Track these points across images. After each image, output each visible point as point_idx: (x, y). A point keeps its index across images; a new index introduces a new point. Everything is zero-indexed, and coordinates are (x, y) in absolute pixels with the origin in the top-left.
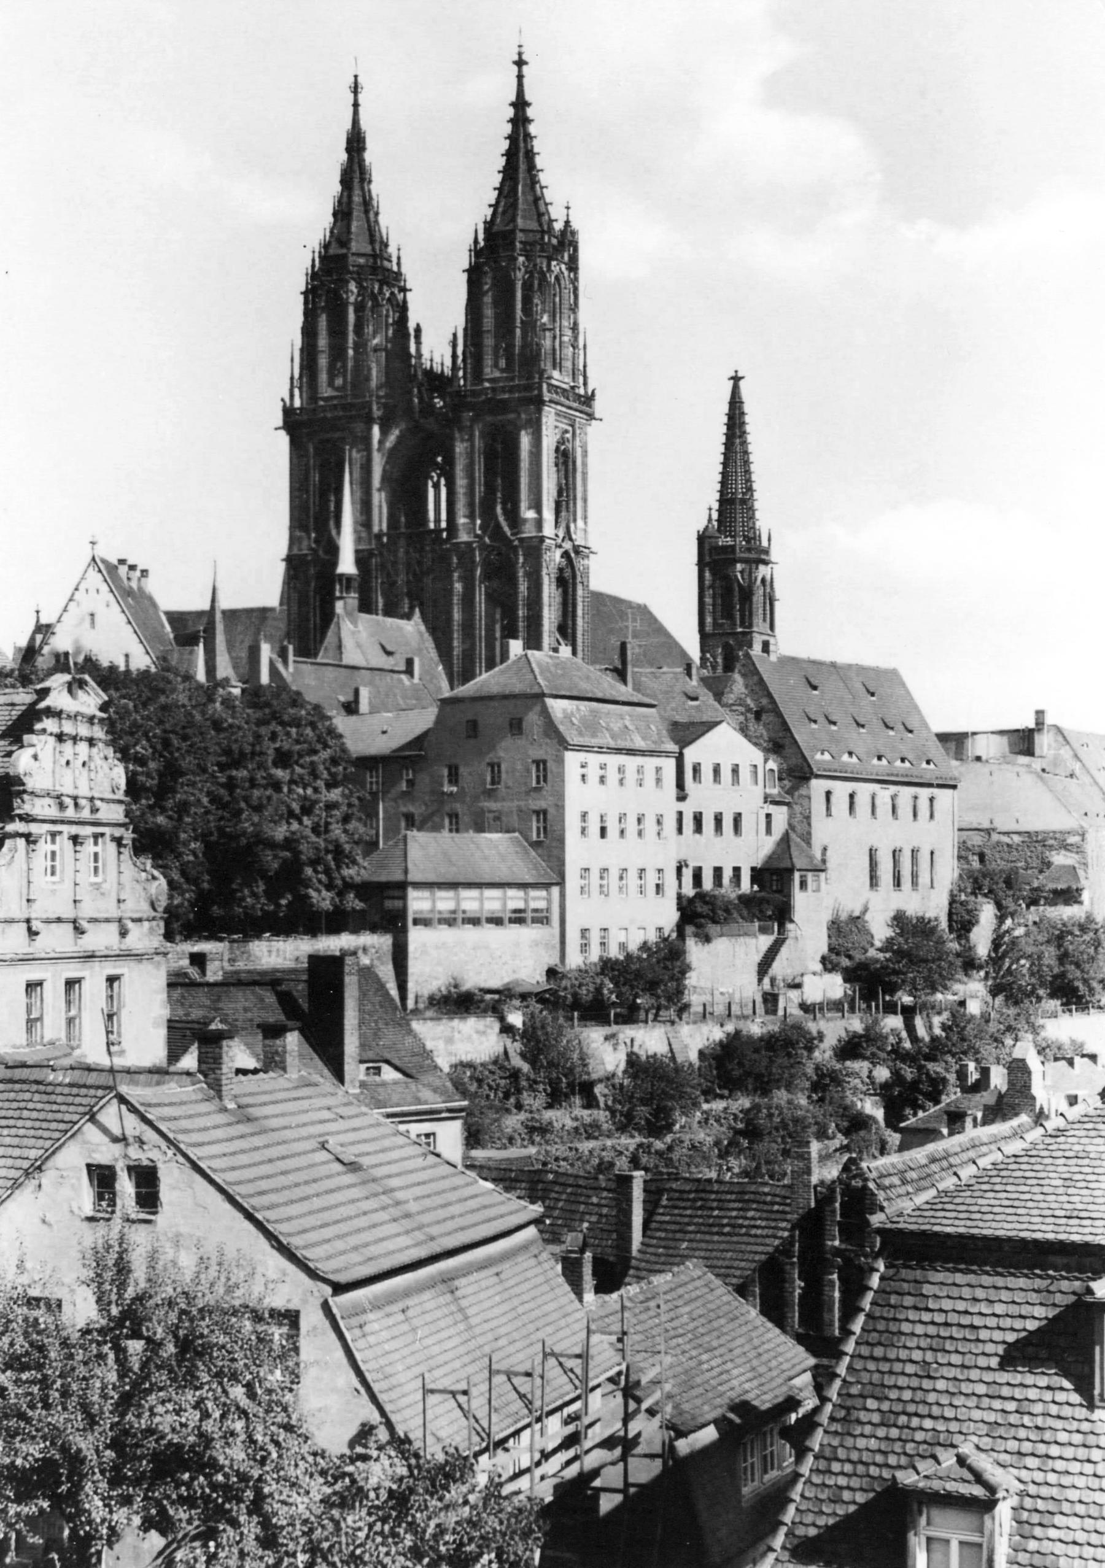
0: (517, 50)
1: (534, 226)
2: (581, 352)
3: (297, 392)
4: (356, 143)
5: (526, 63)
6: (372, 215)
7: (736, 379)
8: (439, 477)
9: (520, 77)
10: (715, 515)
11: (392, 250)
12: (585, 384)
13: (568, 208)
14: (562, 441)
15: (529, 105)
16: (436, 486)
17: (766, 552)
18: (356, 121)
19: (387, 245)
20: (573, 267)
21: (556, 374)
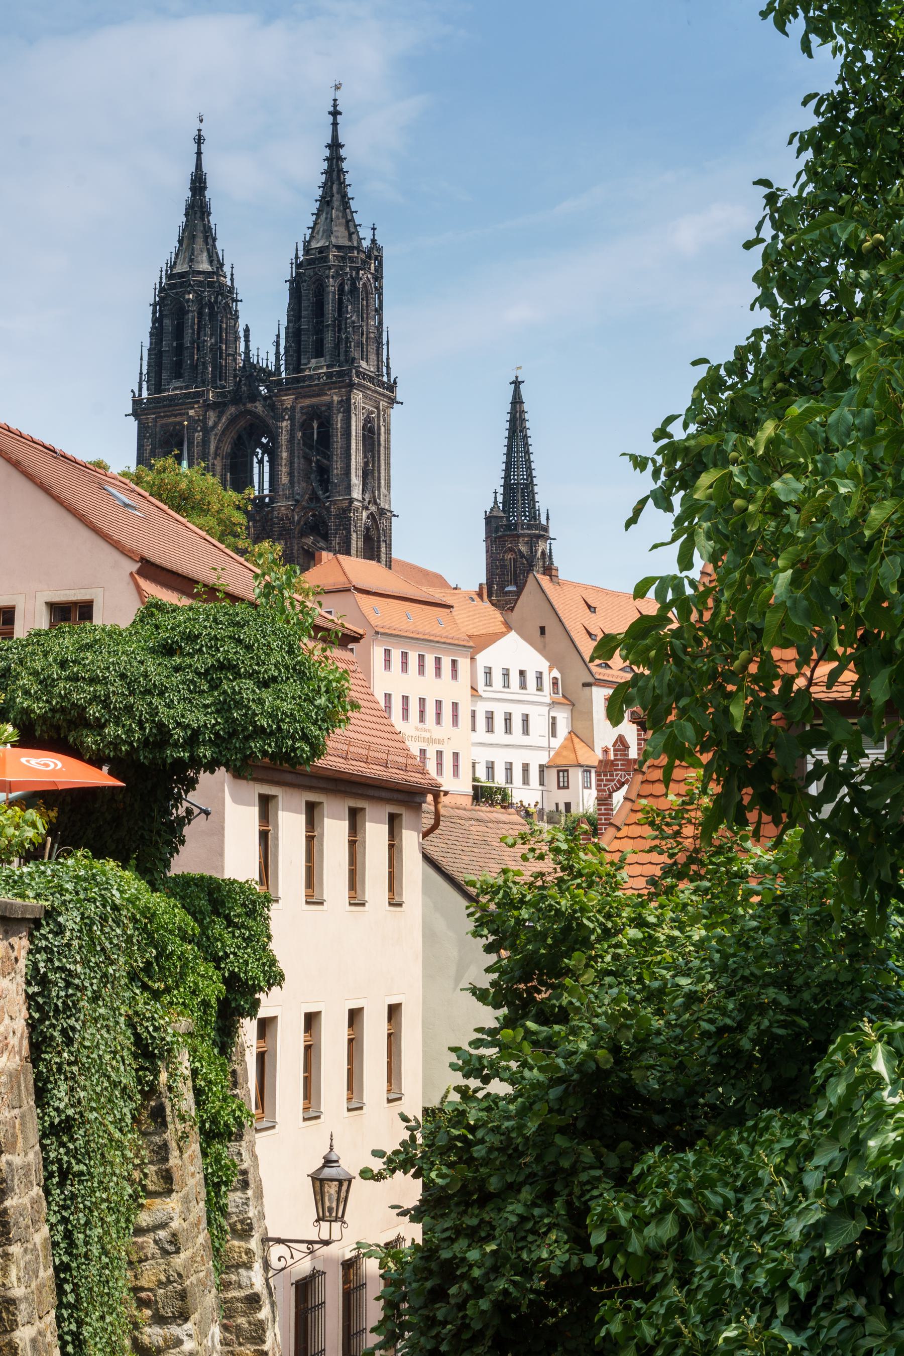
1: (345, 242)
2: (385, 347)
3: (145, 385)
4: (198, 184)
5: (340, 113)
6: (210, 241)
7: (517, 383)
8: (263, 454)
9: (335, 124)
10: (500, 499)
11: (227, 269)
12: (388, 374)
13: (374, 229)
14: (368, 420)
15: (342, 146)
16: (261, 462)
17: (546, 529)
18: (199, 166)
19: (222, 265)
20: (378, 277)
21: (363, 364)
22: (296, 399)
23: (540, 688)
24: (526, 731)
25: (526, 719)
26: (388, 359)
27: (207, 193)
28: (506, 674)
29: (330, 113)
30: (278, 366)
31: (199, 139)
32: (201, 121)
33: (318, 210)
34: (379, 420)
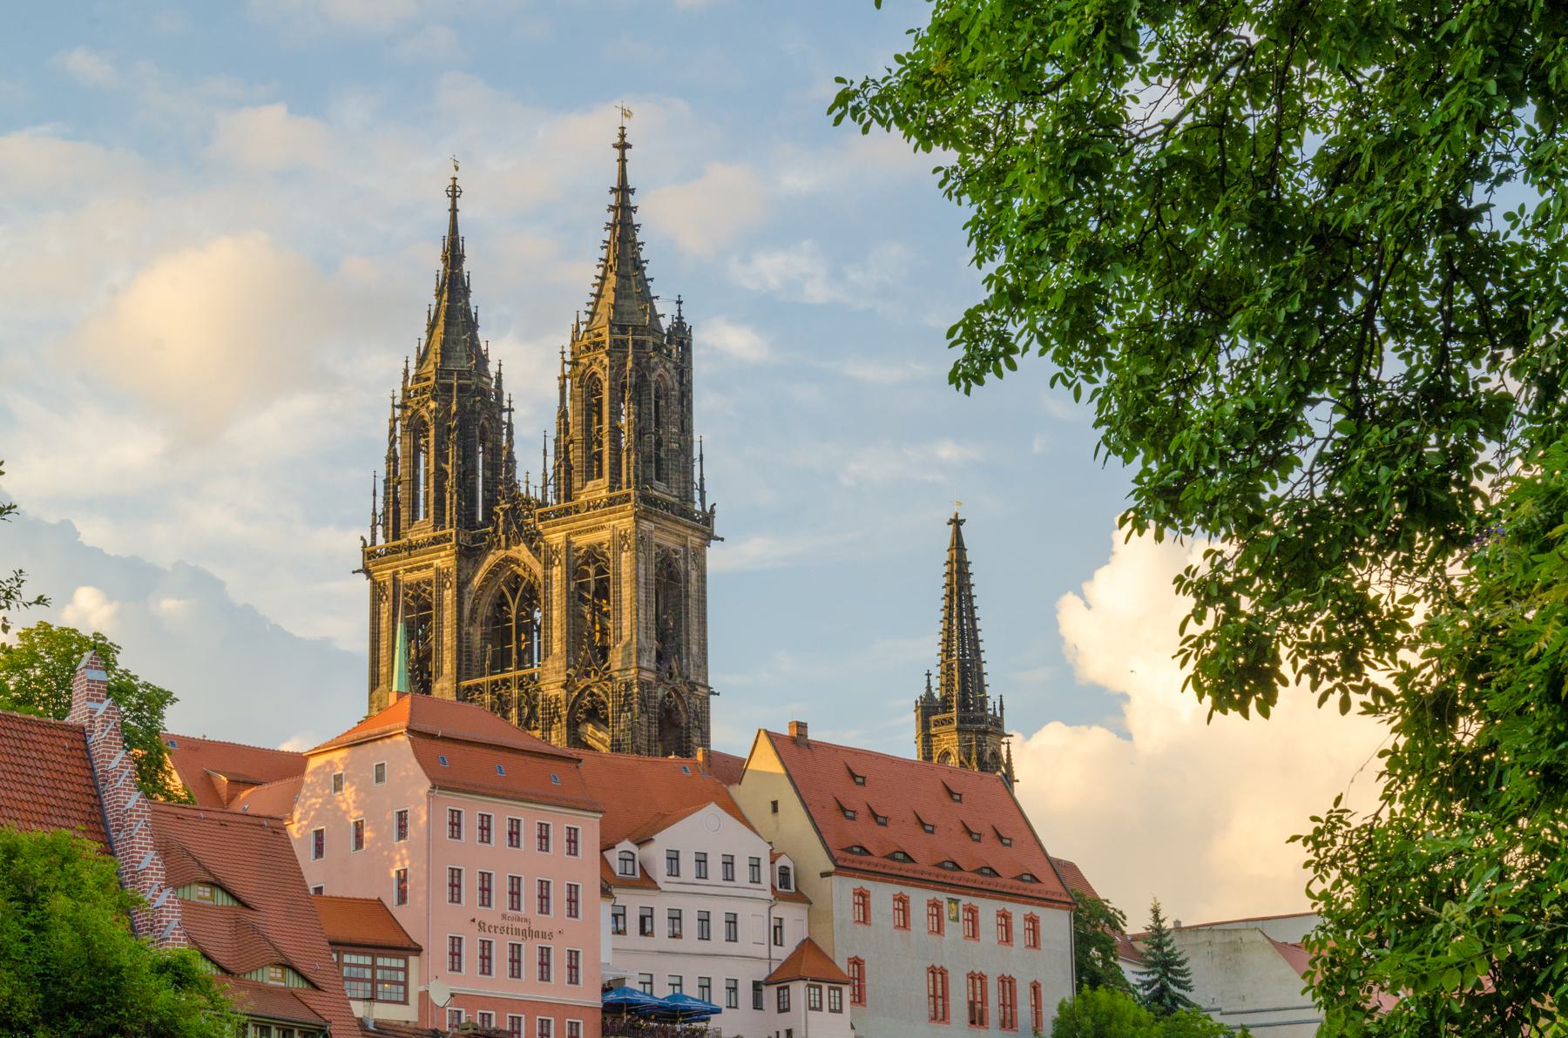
0: (620, 131)
2: (697, 464)
3: (380, 529)
4: (454, 254)
9: (623, 160)
10: (936, 683)
11: (492, 368)
13: (679, 302)
15: (632, 191)
23: (756, 879)
24: (732, 937)
25: (732, 921)
26: (702, 479)
27: (466, 266)
28: (702, 860)
29: (615, 146)
30: (545, 496)
31: (454, 191)
32: (457, 169)
33: (648, 288)
34: (686, 563)
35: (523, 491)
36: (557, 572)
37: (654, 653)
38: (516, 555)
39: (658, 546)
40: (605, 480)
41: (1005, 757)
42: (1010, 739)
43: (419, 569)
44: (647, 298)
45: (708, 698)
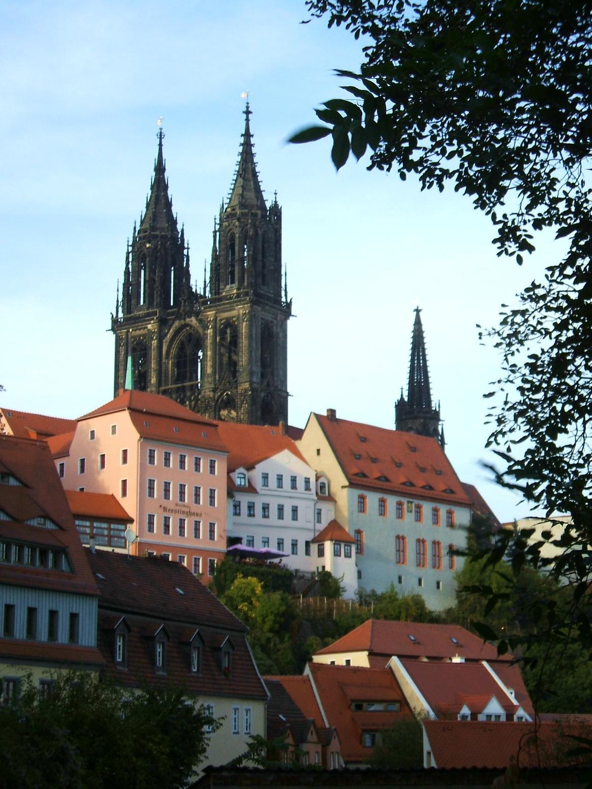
0: (246, 105)
3: (120, 309)
4: (160, 169)
5: (251, 112)
9: (247, 120)
10: (406, 394)
11: (179, 227)
12: (286, 295)
13: (276, 194)
15: (252, 136)
22: (216, 313)
24: (295, 518)
25: (295, 510)
26: (286, 285)
27: (166, 174)
29: (244, 112)
31: (161, 135)
35: (194, 290)
36: (210, 331)
37: (260, 374)
38: (190, 323)
39: (263, 319)
40: (235, 285)
41: (440, 432)
42: (444, 423)
43: (140, 329)
44: (258, 192)
45: (287, 398)
